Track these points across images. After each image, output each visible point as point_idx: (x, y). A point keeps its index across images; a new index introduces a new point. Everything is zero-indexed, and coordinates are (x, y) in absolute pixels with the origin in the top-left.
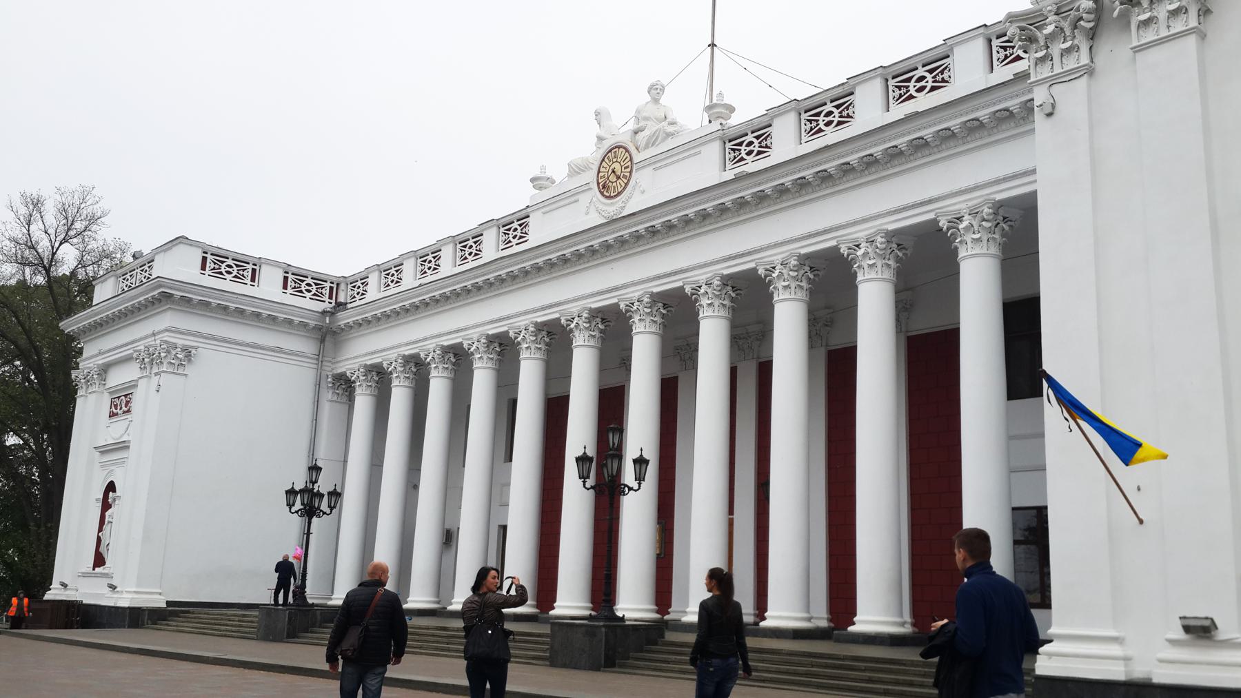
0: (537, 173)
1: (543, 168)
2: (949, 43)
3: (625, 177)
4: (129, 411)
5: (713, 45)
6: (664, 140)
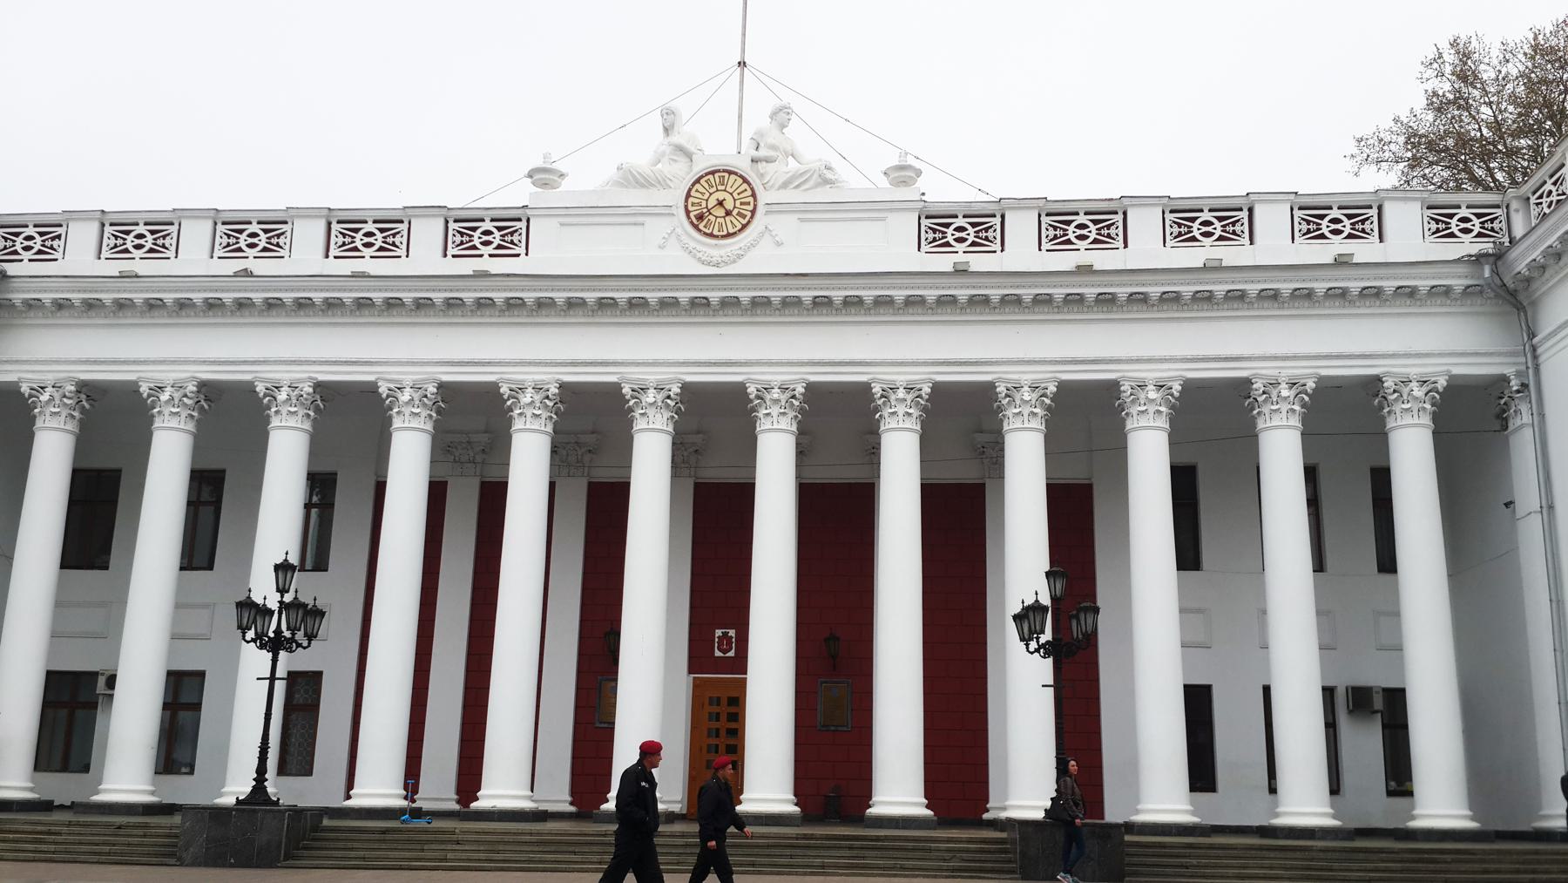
0: (539, 163)
2: (1252, 197)
3: (744, 216)
6: (817, 185)
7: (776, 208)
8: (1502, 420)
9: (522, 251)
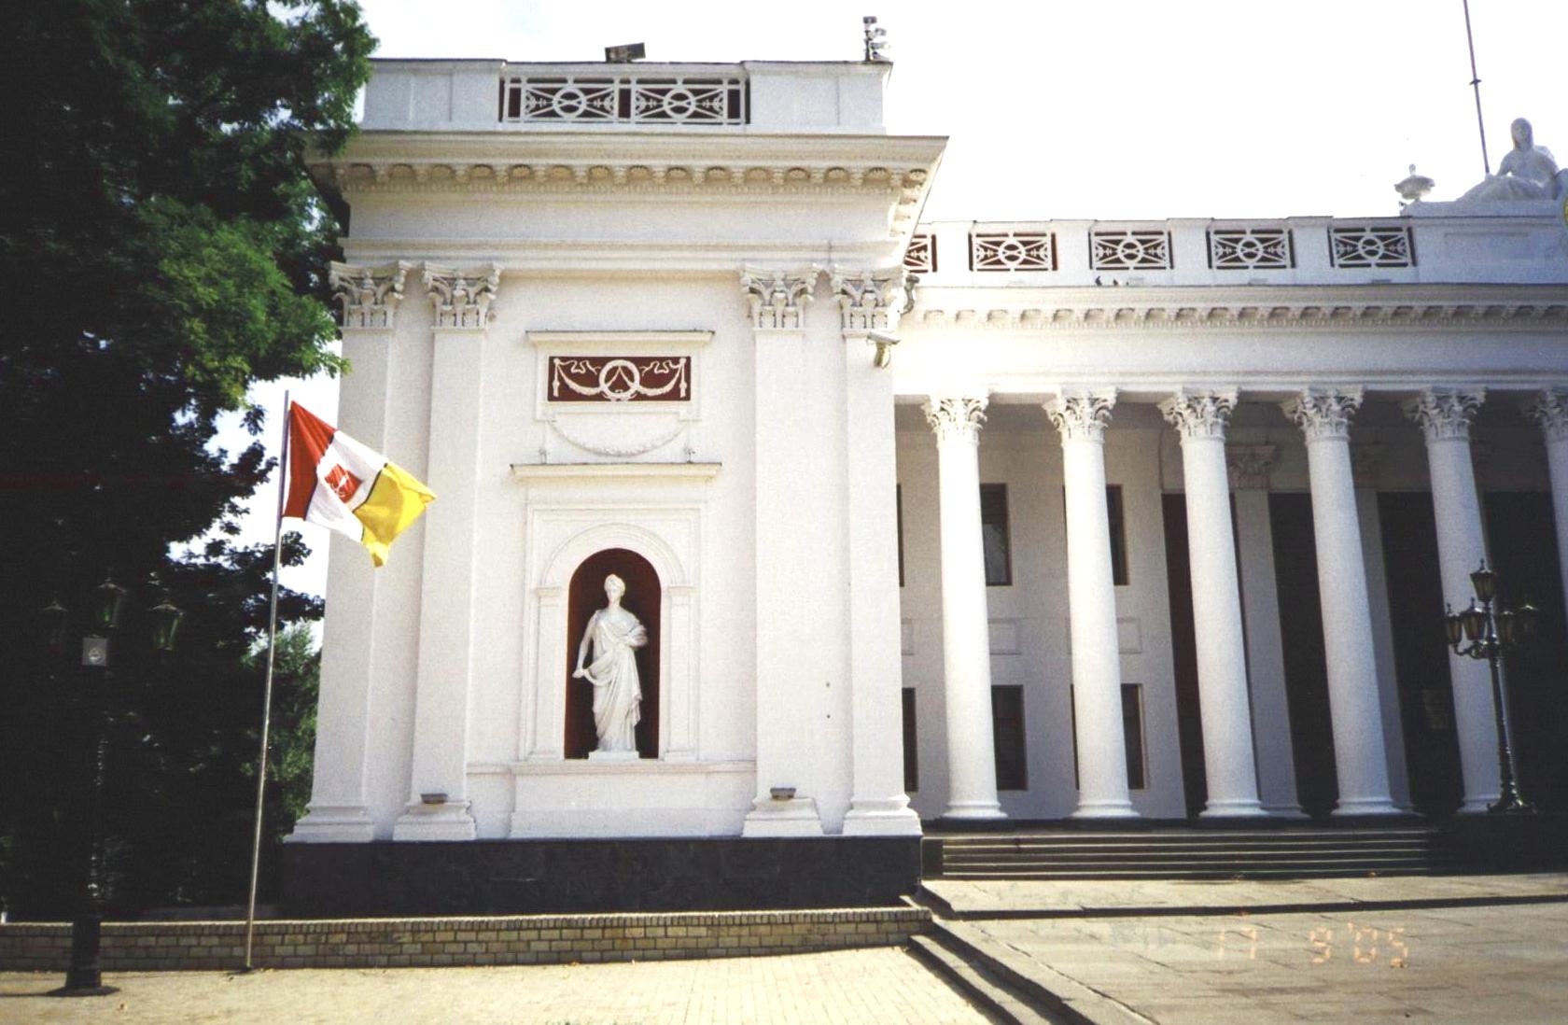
0: (1407, 175)
1: (1412, 168)
4: (673, 395)
5: (1476, 82)
9: (1407, 259)
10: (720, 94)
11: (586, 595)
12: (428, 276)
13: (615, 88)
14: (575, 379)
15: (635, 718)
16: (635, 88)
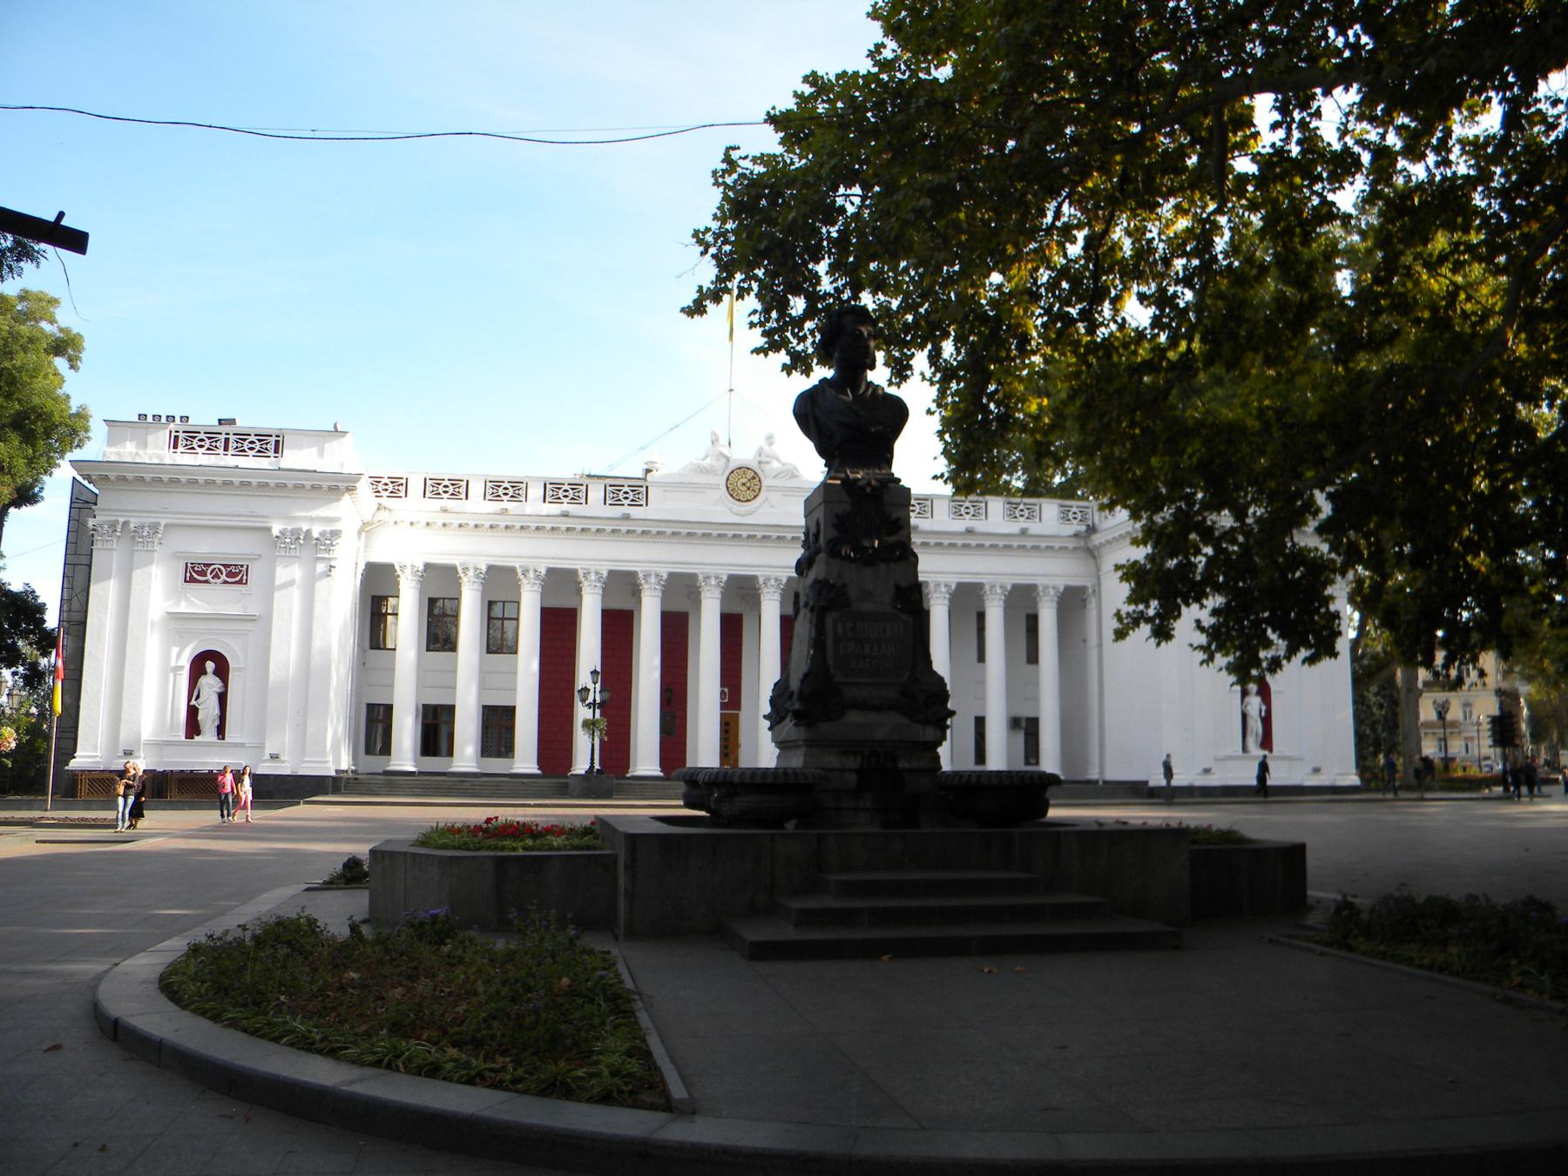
4: (240, 582)
7: (771, 488)
8: (1084, 602)
10: (270, 443)
11: (197, 668)
12: (132, 526)
13: (222, 437)
14: (196, 573)
15: (217, 723)
16: (232, 438)
